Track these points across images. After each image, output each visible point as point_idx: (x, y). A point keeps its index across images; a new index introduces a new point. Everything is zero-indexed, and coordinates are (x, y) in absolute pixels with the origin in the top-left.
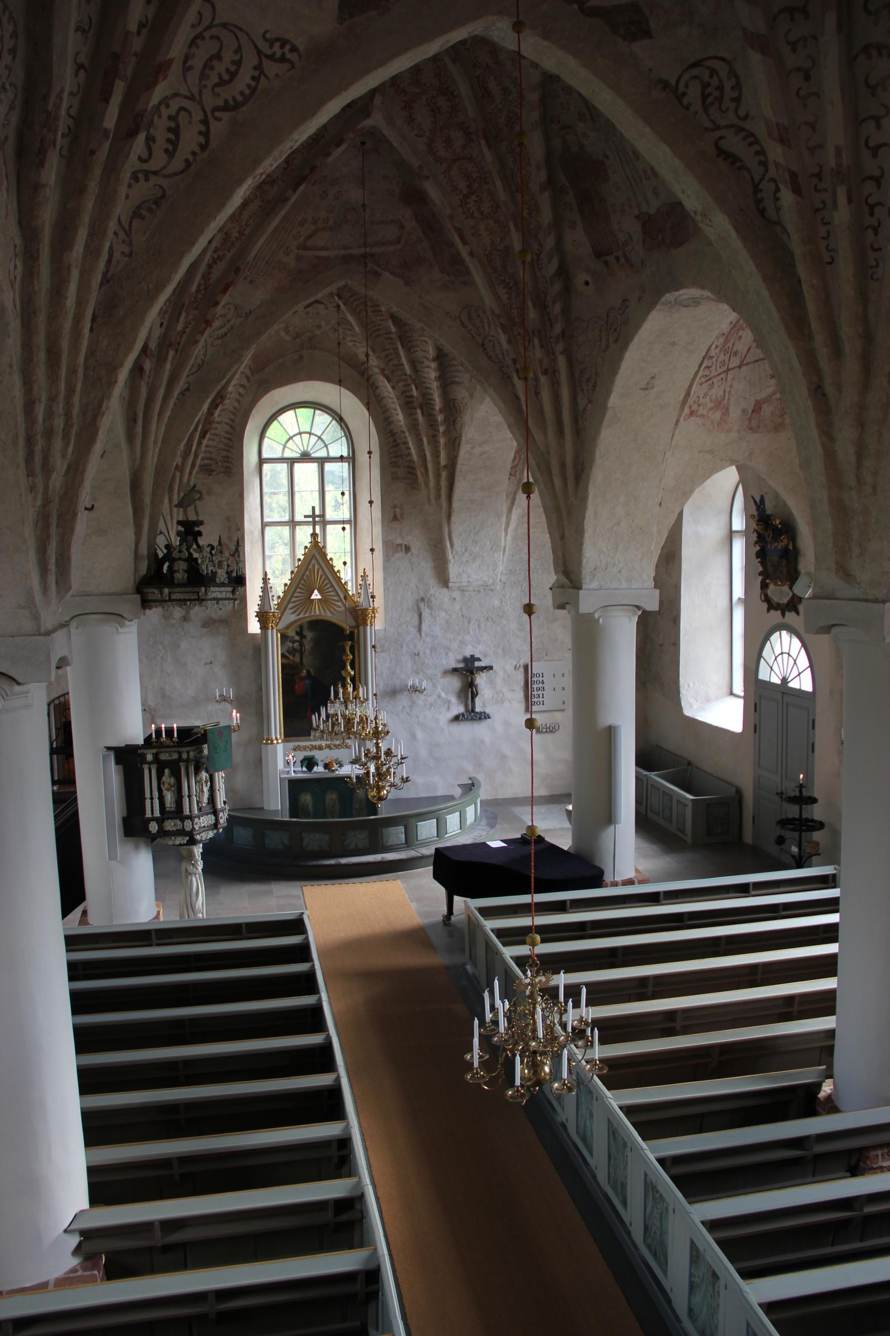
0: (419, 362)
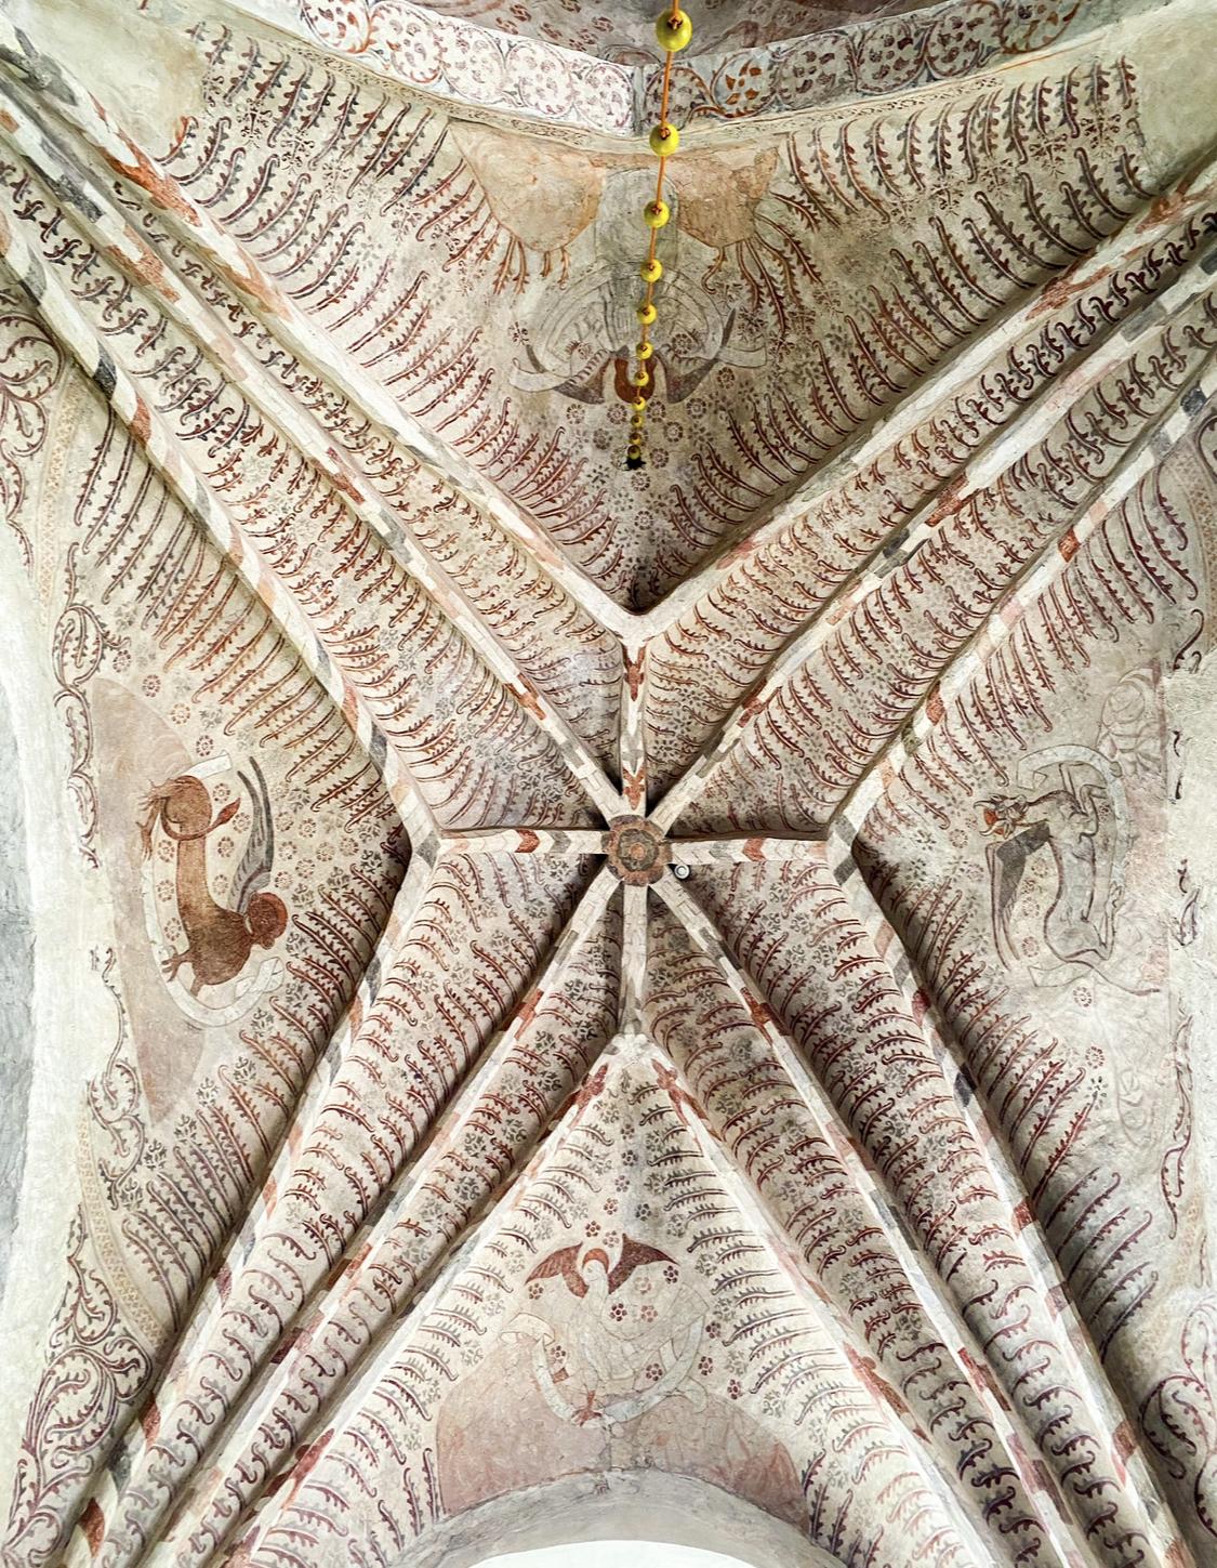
0: (980, 1300)
